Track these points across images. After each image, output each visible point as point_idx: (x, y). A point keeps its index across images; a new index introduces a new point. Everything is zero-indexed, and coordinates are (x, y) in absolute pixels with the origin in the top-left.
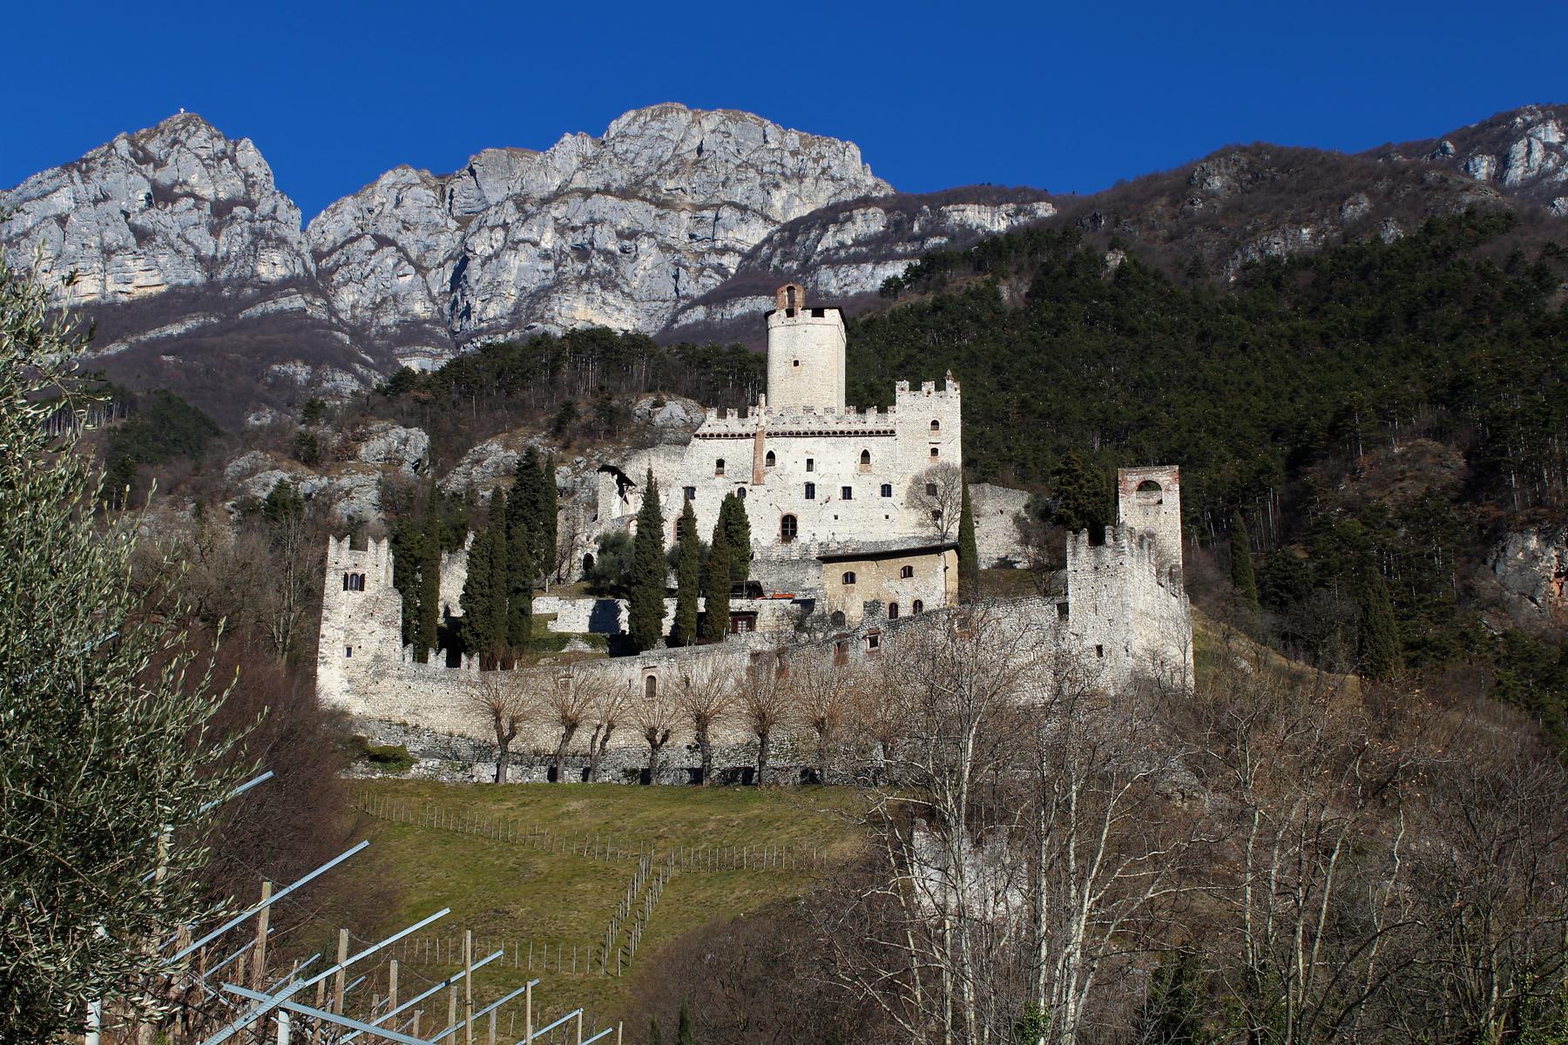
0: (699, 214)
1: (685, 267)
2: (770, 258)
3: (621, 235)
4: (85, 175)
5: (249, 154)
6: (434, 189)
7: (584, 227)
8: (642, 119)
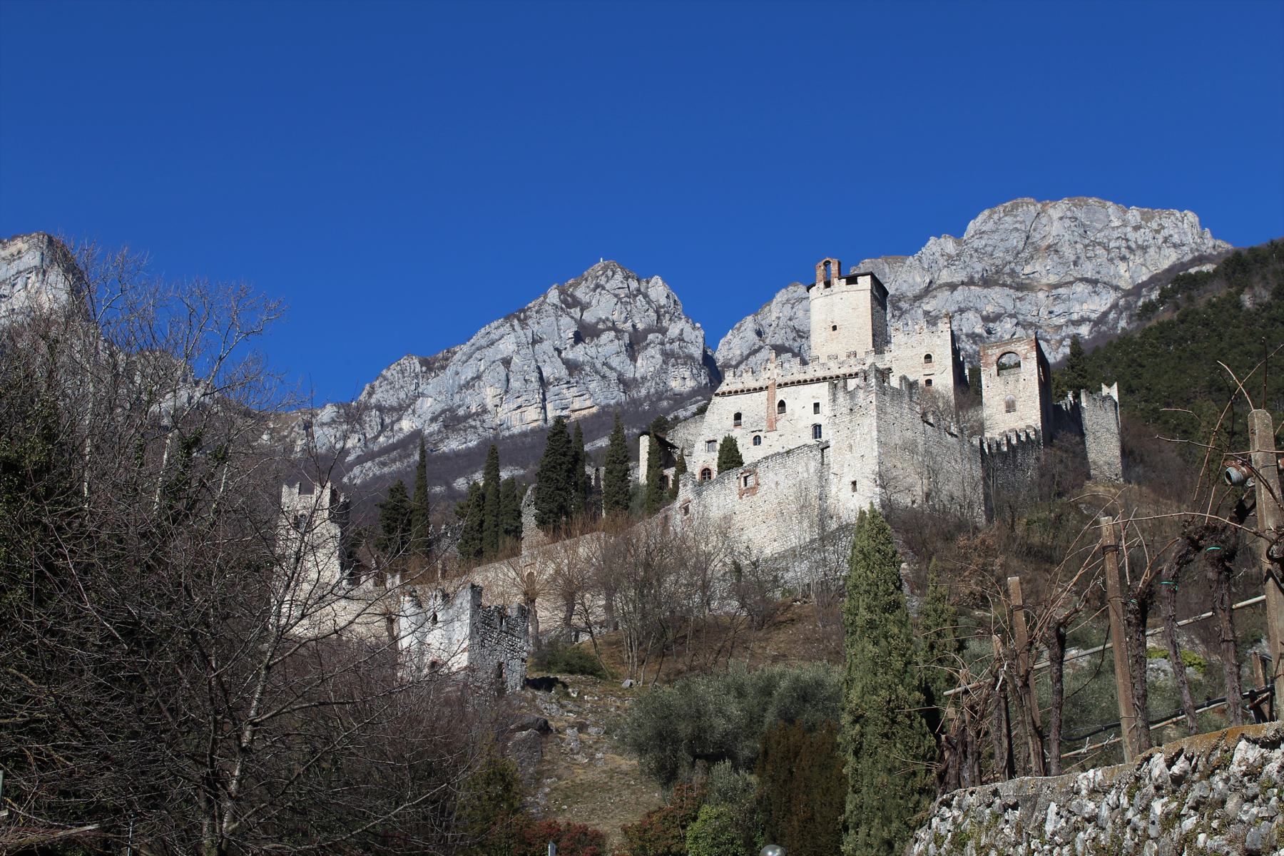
0: (1054, 292)
1: (1047, 341)
2: (1117, 321)
3: (986, 319)
4: (523, 323)
5: (658, 289)
8: (996, 217)
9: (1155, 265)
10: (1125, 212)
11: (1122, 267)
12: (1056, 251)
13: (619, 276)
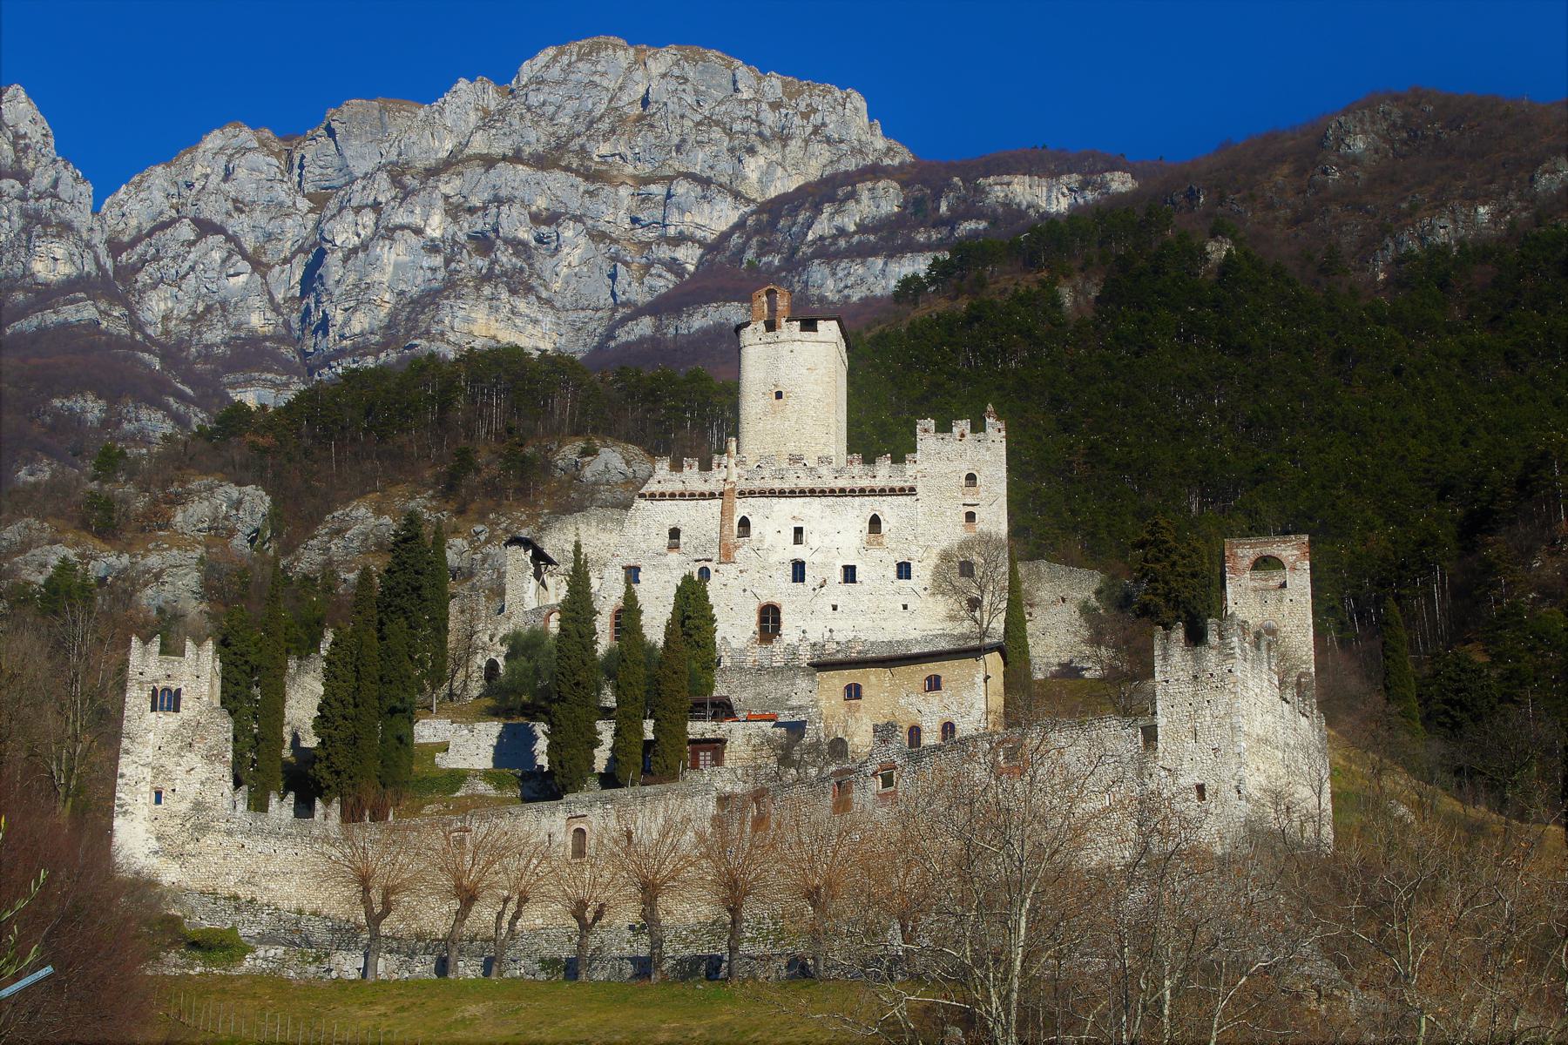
0: (643, 190)
1: (626, 264)
2: (742, 250)
3: (536, 218)
6: (278, 155)
7: (485, 208)
8: (565, 59)
12: (652, 126)
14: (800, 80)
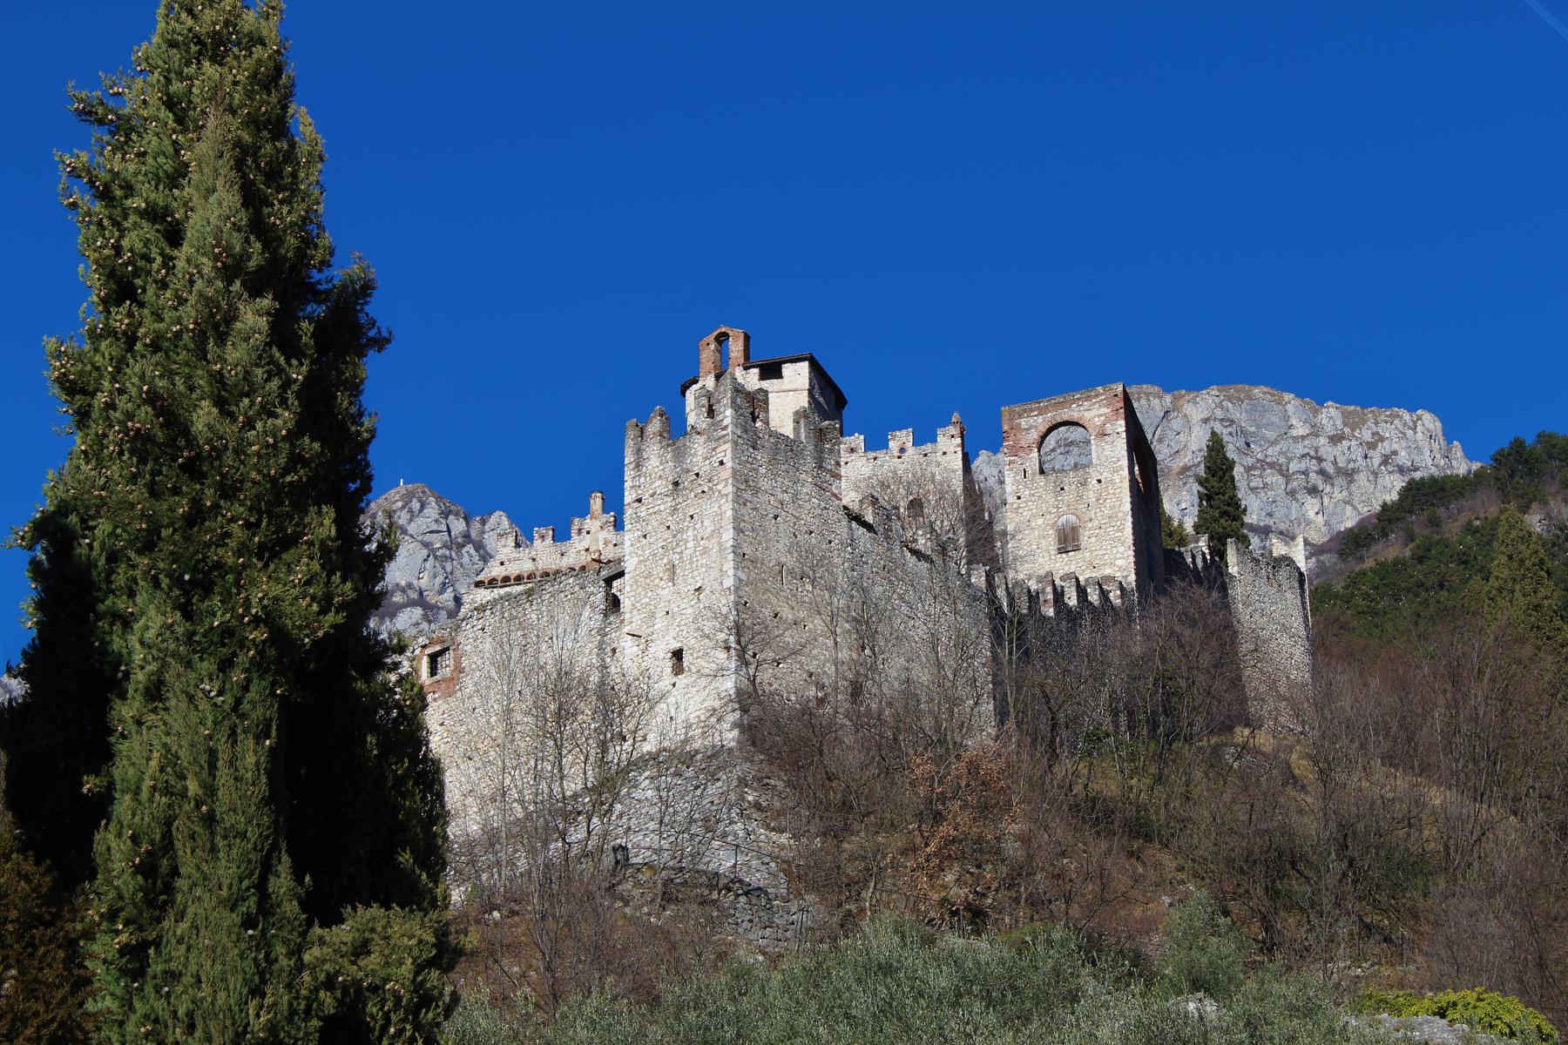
9: (1368, 502)
10: (1316, 412)
11: (1311, 506)
13: (432, 511)
14: (1363, 407)
